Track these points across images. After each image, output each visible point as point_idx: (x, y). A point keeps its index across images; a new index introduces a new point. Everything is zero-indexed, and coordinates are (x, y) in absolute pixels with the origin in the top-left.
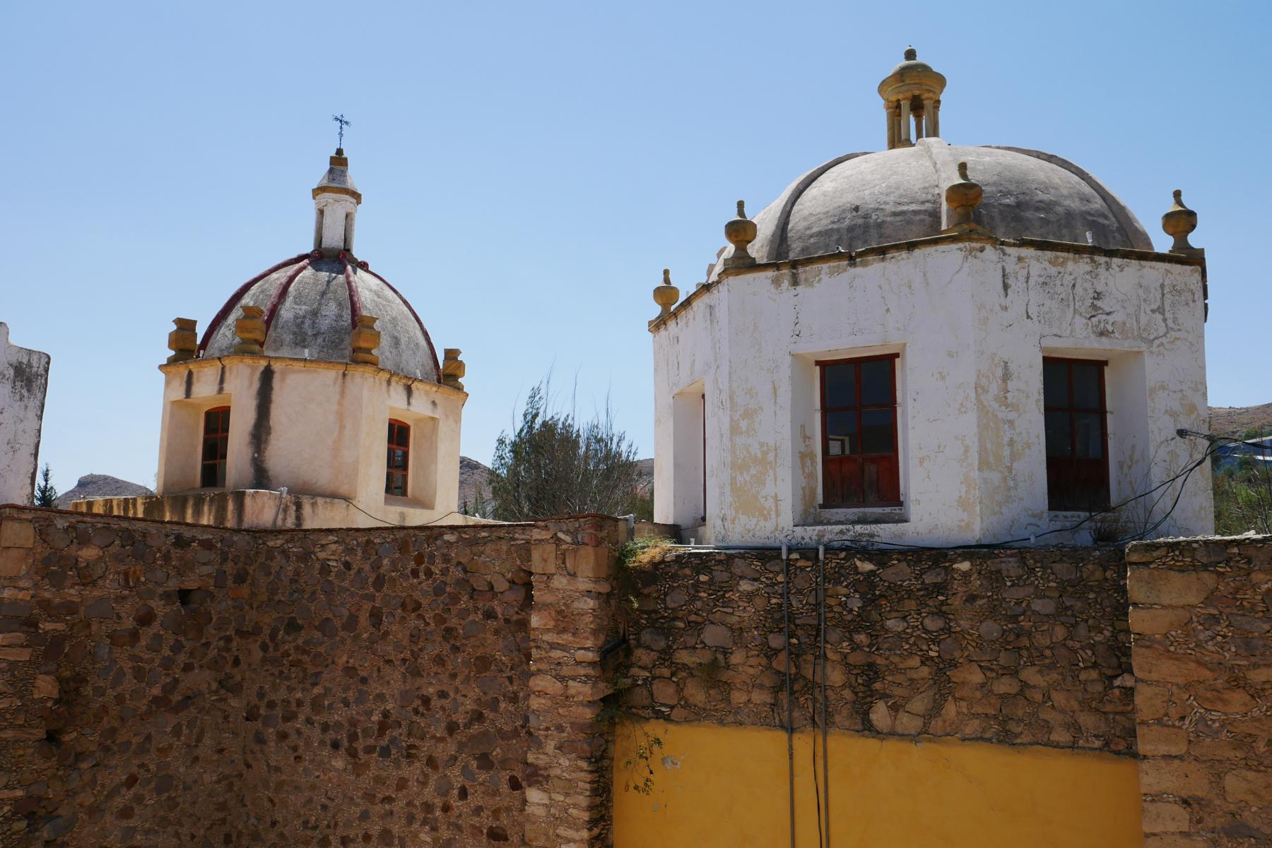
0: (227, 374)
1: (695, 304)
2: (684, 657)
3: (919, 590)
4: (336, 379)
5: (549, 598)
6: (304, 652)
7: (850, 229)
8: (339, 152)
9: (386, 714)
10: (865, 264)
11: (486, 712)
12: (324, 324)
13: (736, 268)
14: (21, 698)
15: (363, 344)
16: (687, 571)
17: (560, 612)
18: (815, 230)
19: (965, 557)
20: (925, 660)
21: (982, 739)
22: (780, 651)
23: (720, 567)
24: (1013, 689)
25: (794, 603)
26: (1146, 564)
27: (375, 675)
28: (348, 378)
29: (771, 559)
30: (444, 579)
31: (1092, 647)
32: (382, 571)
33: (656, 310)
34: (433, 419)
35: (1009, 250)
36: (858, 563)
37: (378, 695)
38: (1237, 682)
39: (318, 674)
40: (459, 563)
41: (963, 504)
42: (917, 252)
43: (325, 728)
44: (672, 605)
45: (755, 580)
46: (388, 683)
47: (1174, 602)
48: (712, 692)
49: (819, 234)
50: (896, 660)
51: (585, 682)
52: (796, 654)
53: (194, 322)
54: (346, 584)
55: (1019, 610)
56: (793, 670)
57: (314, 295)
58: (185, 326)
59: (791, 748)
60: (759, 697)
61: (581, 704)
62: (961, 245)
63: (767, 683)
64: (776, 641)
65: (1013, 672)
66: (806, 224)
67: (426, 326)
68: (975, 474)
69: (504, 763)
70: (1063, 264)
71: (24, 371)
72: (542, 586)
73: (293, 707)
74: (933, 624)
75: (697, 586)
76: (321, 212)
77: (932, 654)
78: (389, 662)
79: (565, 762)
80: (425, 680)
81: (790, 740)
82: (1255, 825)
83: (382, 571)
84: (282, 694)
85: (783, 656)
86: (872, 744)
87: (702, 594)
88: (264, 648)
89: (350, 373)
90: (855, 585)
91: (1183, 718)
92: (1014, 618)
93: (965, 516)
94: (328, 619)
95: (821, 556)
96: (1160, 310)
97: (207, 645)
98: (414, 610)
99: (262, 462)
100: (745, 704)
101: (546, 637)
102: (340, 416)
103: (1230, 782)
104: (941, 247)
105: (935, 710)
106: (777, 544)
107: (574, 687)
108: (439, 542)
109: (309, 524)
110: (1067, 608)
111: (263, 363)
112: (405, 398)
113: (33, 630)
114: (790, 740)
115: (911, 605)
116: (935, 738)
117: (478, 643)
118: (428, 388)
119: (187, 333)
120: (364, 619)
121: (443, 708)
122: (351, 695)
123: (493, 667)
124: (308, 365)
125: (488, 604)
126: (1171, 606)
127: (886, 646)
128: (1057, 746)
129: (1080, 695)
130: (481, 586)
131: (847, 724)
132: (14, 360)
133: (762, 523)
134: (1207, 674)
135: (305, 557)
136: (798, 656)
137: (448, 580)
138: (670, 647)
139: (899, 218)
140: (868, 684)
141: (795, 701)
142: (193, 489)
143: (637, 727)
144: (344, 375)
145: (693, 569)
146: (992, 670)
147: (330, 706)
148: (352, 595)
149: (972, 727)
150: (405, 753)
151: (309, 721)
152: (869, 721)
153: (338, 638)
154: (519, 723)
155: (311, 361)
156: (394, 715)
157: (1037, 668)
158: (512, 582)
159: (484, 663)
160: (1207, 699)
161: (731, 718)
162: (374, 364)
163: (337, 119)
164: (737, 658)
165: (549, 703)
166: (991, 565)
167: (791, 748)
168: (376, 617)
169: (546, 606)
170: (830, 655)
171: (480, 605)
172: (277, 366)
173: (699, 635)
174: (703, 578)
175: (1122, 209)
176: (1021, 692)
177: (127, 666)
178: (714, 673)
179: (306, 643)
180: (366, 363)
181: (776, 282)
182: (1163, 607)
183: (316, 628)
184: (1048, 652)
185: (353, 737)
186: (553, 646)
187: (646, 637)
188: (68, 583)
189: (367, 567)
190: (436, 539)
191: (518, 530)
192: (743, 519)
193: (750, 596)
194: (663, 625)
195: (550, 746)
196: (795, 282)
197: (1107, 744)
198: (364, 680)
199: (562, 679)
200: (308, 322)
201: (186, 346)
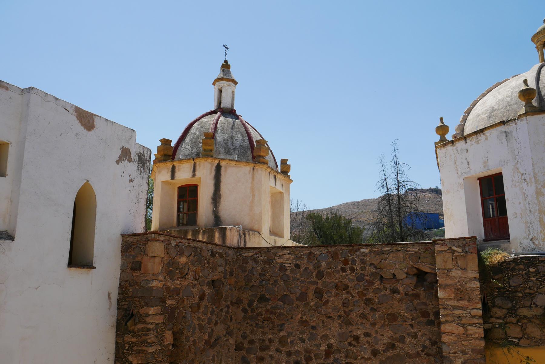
0: (197, 167)
1: (487, 132)
2: (524, 312)
5: (449, 282)
6: (272, 313)
8: (226, 62)
9: (330, 346)
11: (397, 344)
12: (238, 144)
14: (160, 345)
17: (458, 289)
23: (542, 264)
27: (321, 324)
28: (255, 170)
32: (321, 269)
33: (438, 138)
34: (281, 193)
37: (323, 336)
39: (282, 325)
40: (371, 264)
43: (289, 354)
44: (514, 285)
46: (330, 329)
51: (479, 327)
53: (171, 141)
54: (298, 276)
57: (229, 129)
61: (476, 339)
71: (142, 158)
72: (445, 275)
73: (267, 343)
75: (528, 274)
76: (220, 91)
78: (330, 317)
80: (354, 327)
83: (321, 269)
84: (258, 336)
87: (533, 279)
88: (245, 311)
94: (286, 295)
97: (222, 310)
98: (344, 290)
99: (218, 212)
101: (449, 303)
102: (253, 190)
107: (472, 330)
108: (358, 253)
109: (249, 245)
111: (217, 162)
113: (164, 304)
120: (311, 294)
121: (368, 342)
122: (305, 336)
123: (399, 319)
124: (237, 163)
132: (138, 151)
135: (269, 262)
137: (366, 273)
138: (515, 307)
142: (172, 227)
144: (253, 169)
147: (292, 342)
148: (302, 282)
151: (277, 350)
153: (294, 305)
154: (419, 349)
158: (407, 273)
159: (393, 317)
163: (224, 46)
168: (319, 293)
171: (388, 286)
172: (223, 164)
173: (532, 300)
174: (532, 270)
177: (196, 323)
179: (272, 308)
180: (264, 163)
183: (279, 300)
186: (455, 308)
187: (498, 301)
188: (176, 277)
189: (311, 267)
190: (356, 251)
191: (410, 246)
198: (314, 328)
199: (463, 325)
200: (230, 143)
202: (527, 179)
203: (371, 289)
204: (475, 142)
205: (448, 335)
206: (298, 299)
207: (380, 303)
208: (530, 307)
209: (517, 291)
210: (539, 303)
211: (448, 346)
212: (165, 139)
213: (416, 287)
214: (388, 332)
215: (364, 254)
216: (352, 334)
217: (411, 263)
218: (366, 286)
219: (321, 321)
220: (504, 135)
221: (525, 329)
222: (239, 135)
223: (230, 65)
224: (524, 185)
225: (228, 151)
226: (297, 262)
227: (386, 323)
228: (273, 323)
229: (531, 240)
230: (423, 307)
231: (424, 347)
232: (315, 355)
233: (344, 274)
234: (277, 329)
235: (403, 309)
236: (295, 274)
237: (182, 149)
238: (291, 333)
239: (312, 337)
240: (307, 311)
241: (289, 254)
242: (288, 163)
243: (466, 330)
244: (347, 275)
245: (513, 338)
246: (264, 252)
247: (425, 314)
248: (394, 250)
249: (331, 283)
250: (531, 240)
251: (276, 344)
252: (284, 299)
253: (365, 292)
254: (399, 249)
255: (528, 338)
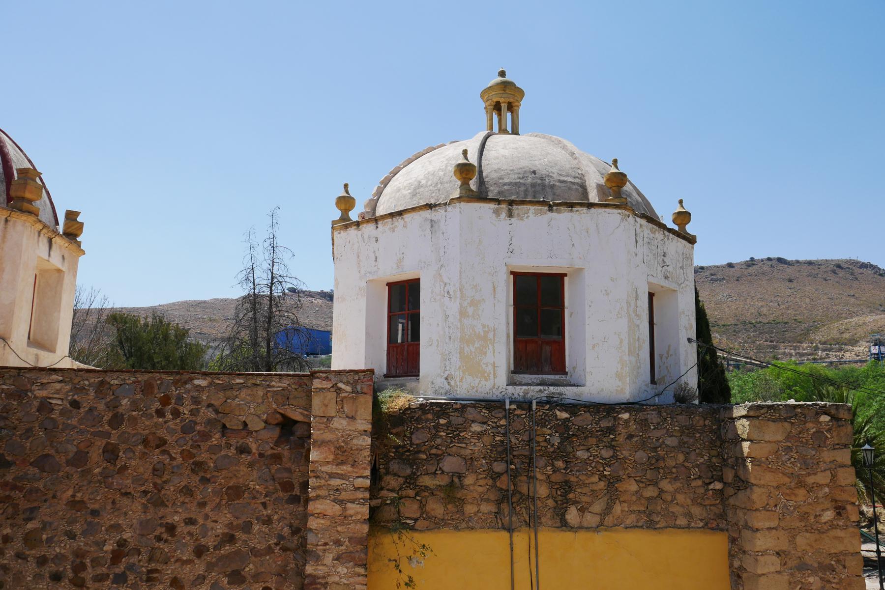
1: (407, 217)
2: (426, 481)
3: (597, 431)
5: (328, 436)
6: (14, 488)
7: (533, 185)
9: (122, 543)
10: (559, 212)
11: (238, 534)
13: (468, 197)
16: (430, 416)
17: (339, 448)
18: (506, 180)
19: (627, 410)
20: (602, 477)
21: (637, 526)
22: (502, 474)
23: (456, 414)
24: (655, 494)
25: (513, 440)
26: (757, 417)
28: (10, 224)
29: (496, 408)
30: (194, 418)
31: (698, 466)
32: (121, 410)
33: (337, 214)
35: (638, 219)
36: (558, 413)
37: (111, 526)
38: (801, 484)
39: (32, 510)
41: (619, 376)
42: (593, 210)
43: (42, 561)
45: (484, 423)
46: (126, 514)
47: (771, 439)
48: (450, 506)
49: (510, 184)
50: (583, 478)
51: (363, 504)
52: (514, 476)
54: (74, 421)
55: (658, 444)
56: (512, 487)
59: (511, 544)
60: (486, 508)
61: (357, 522)
62: (620, 211)
63: (492, 496)
64: (499, 467)
65: (654, 483)
66: (498, 175)
68: (626, 358)
69: (256, 577)
70: (654, 233)
72: (323, 426)
74: (606, 453)
75: (437, 427)
77: (606, 473)
78: (127, 494)
79: (342, 570)
80: (169, 509)
81: (511, 537)
82: (810, 563)
83: (121, 410)
85: (504, 478)
86: (568, 535)
87: (442, 434)
89: (12, 220)
90: (556, 428)
91: (776, 506)
92: (655, 449)
93: (620, 384)
95: (534, 407)
96: (682, 268)
98: (158, 447)
100: (475, 514)
101: (324, 469)
103: (799, 540)
104: (608, 210)
105: (608, 510)
106: (500, 396)
107: (352, 508)
108: (188, 386)
110: (685, 443)
112: (47, 249)
114: (511, 537)
115: (592, 441)
116: (609, 528)
117: (230, 475)
120: (95, 455)
121: (190, 534)
122: (77, 528)
123: (246, 495)
125: (241, 442)
126: (770, 442)
127: (577, 468)
128: (680, 527)
129: (692, 495)
130: (232, 424)
131: (550, 523)
133: (483, 382)
134: (787, 480)
135: (20, 394)
136: (515, 477)
137: (199, 419)
138: (415, 474)
139: (563, 185)
140: (565, 495)
141: (513, 508)
143: (389, 536)
144: (6, 221)
145: (434, 414)
146: (642, 482)
147: (49, 540)
148: (81, 432)
149: (631, 520)
150: (144, 577)
151: (19, 556)
152: (565, 520)
153: (61, 474)
154: (273, 541)
156: (132, 543)
157: (668, 480)
158: (266, 422)
159: (236, 492)
160: (787, 494)
161: (464, 525)
164: (469, 480)
165: (329, 523)
166: (641, 415)
167: (511, 544)
168: (111, 453)
169: (322, 444)
170: (539, 476)
171: (233, 441)
173: (438, 464)
174: (442, 421)
175: (649, 204)
176: (659, 496)
178: (452, 491)
180: (30, 212)
181: (497, 212)
182: (766, 442)
183: (31, 464)
184: (674, 470)
185: (79, 568)
187: (394, 466)
189: (101, 406)
190: (186, 383)
191: (276, 379)
192: (469, 379)
193: (480, 435)
194: (408, 456)
195: (329, 559)
196: (510, 215)
197: (706, 524)
198: (95, 513)
199: (341, 502)
202: (451, 293)
203: (204, 446)
204: (389, 229)
205: (318, 517)
206: (69, 463)
207: (218, 469)
208: (435, 474)
209: (419, 452)
210: (445, 469)
211: (317, 534)
213: (277, 443)
214: (226, 517)
215: (199, 388)
216: (164, 521)
217: (274, 406)
218: (196, 441)
219: (110, 501)
220: (429, 224)
221: (425, 506)
224: (447, 299)
226: (76, 397)
227: (224, 502)
228: (16, 507)
229: (446, 379)
230: (286, 475)
231: (281, 537)
232: (92, 561)
233: (161, 420)
234: (22, 517)
235: (253, 479)
236: (68, 419)
238: (51, 524)
239: (90, 529)
240: (85, 483)
241: (61, 382)
242: (79, 219)
243: (345, 509)
244: (166, 422)
245: (408, 518)
246: (11, 376)
247: (287, 486)
248: (249, 385)
249: (134, 435)
250: (446, 379)
251: (18, 545)
252: (43, 462)
253: (194, 451)
254: (258, 382)
255: (428, 518)
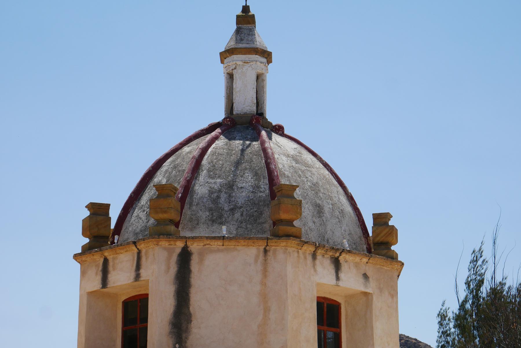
4: (257, 257)
8: (246, 9)
12: (241, 197)
15: (284, 216)
28: (270, 254)
34: (366, 294)
53: (108, 206)
57: (228, 167)
58: (98, 211)
67: (350, 190)
76: (230, 77)
102: (264, 297)
111: (180, 245)
112: (333, 272)
118: (357, 259)
119: (100, 218)
124: (226, 243)
144: (266, 251)
155: (230, 239)
162: (297, 236)
172: (194, 247)
180: (288, 236)
200: (223, 196)
201: (100, 232)
212: (91, 203)
222: (249, 176)
223: (253, 16)
225: (217, 218)
237: (133, 218)
242: (390, 223)
